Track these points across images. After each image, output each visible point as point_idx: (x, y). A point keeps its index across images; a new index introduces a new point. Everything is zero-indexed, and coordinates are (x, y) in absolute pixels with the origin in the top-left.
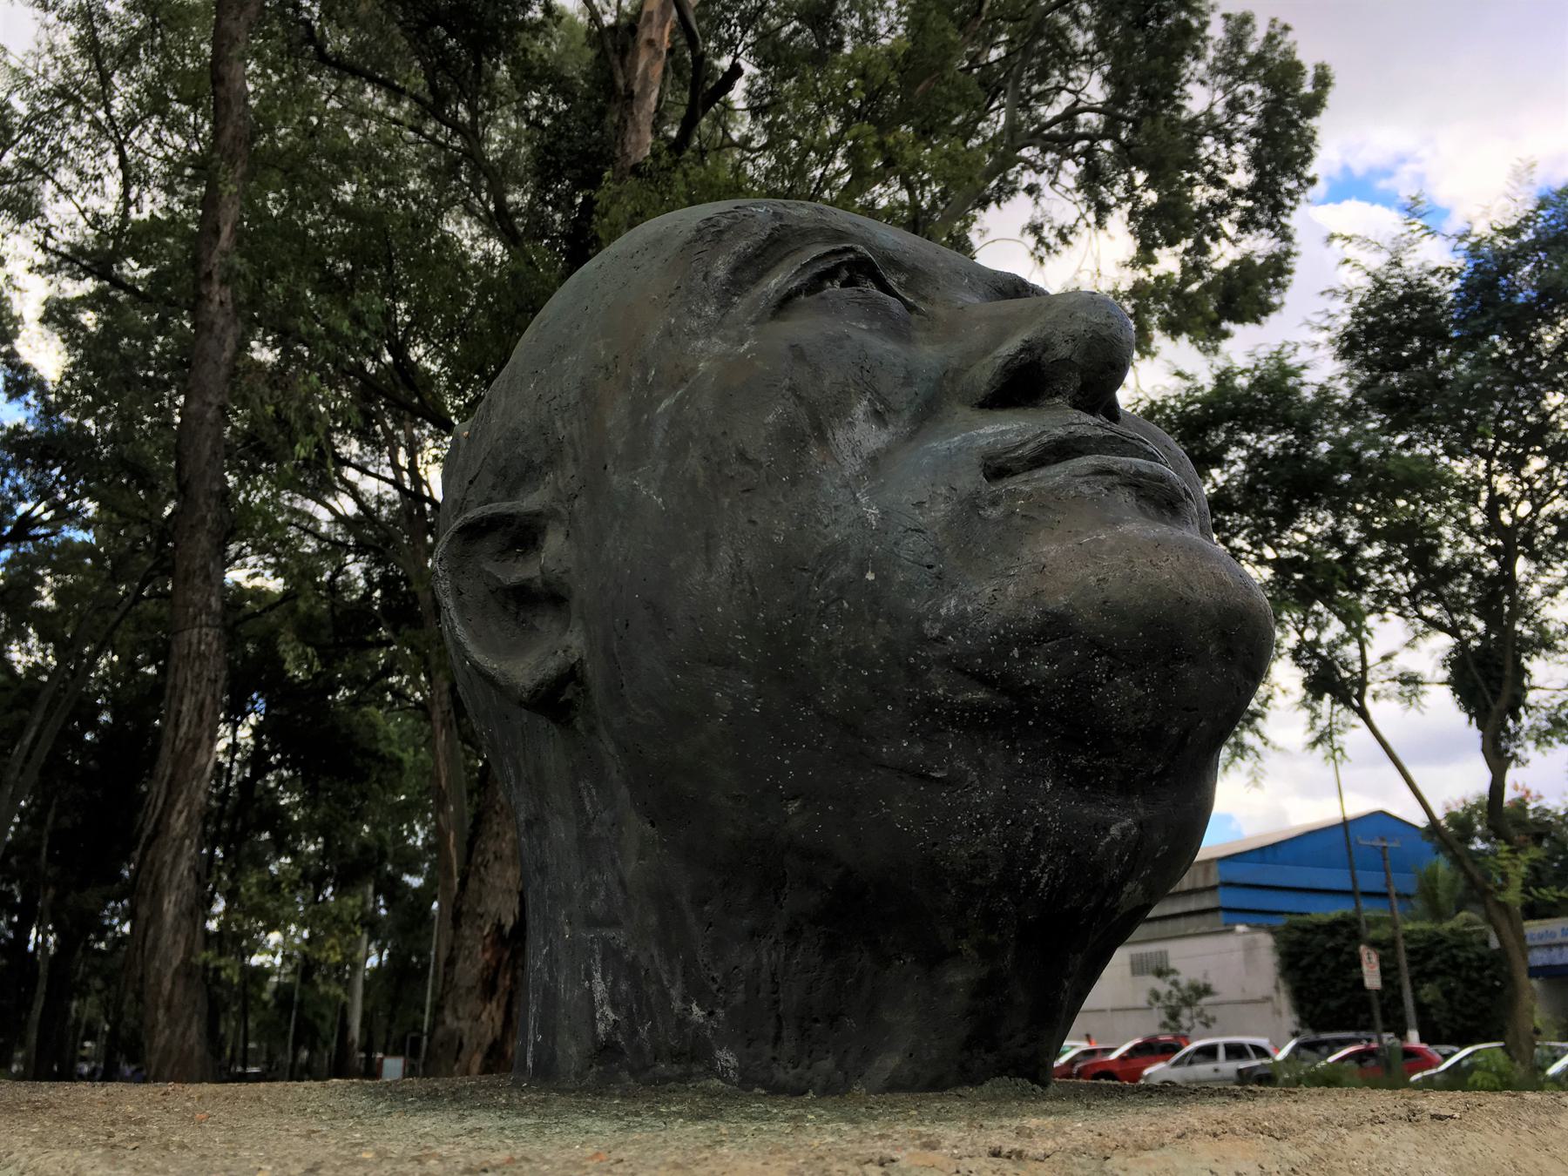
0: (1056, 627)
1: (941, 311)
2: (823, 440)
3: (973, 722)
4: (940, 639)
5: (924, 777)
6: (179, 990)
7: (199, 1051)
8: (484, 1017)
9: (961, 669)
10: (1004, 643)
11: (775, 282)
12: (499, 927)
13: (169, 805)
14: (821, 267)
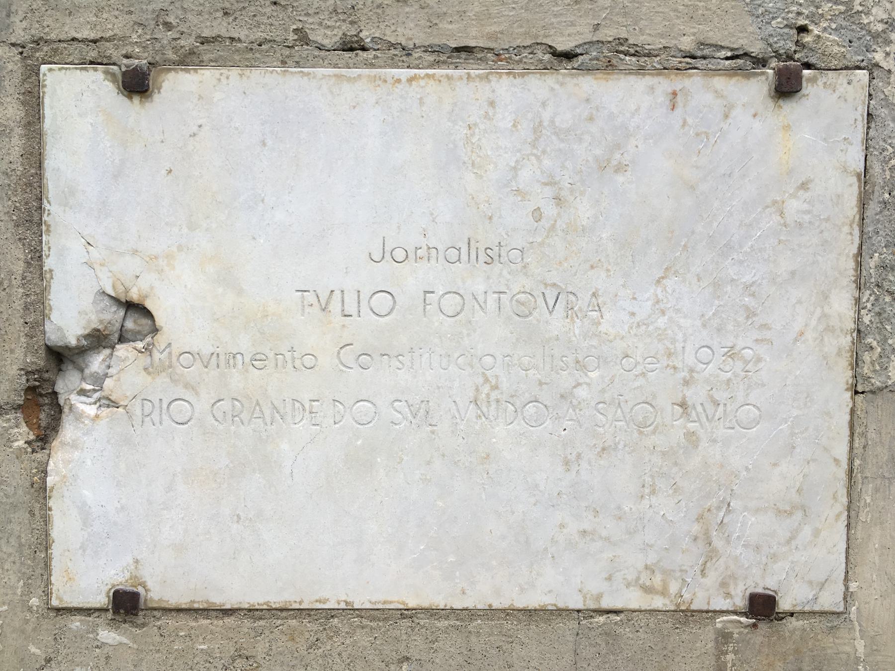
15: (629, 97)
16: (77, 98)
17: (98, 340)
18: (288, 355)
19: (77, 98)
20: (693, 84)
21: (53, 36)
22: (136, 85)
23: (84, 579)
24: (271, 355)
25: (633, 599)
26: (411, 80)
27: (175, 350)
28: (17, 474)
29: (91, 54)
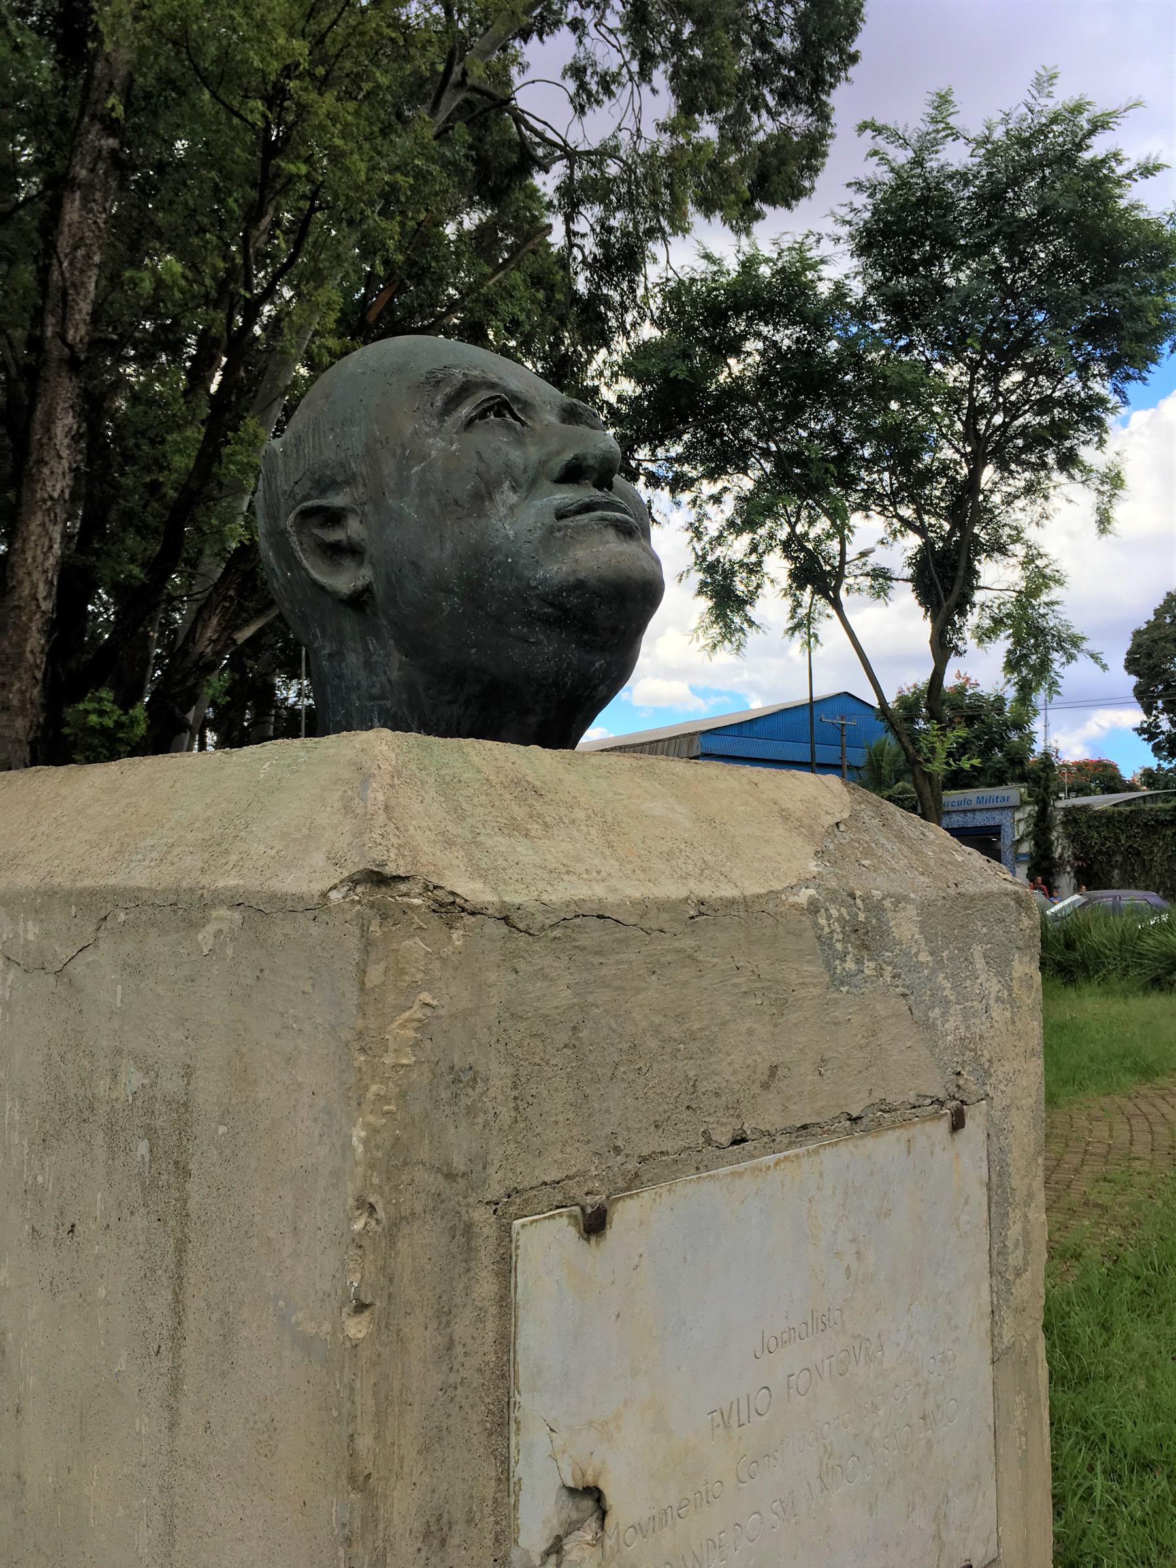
0: (580, 585)
1: (537, 426)
2: (491, 499)
3: (548, 622)
4: (536, 588)
5: (527, 641)
9: (544, 600)
10: (561, 590)
11: (465, 411)
14: (486, 405)
18: (703, 1489)
21: (526, 1184)
22: (594, 1224)
24: (691, 1496)
26: (777, 1164)
27: (622, 1528)
29: (553, 1196)
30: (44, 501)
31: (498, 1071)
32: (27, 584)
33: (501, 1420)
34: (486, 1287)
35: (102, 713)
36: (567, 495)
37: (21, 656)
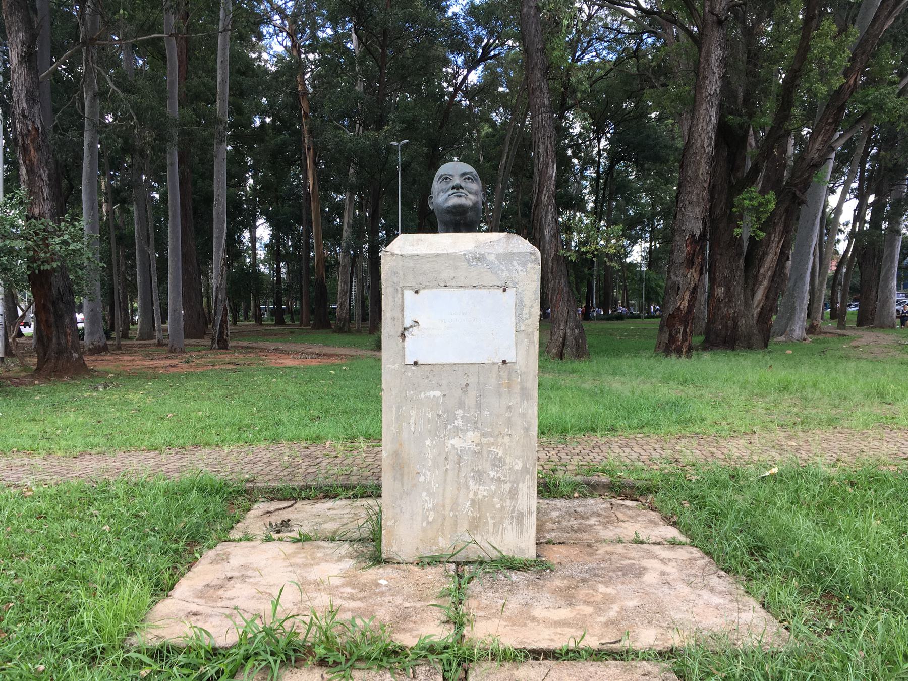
6: (555, 266)
7: (565, 289)
8: (689, 276)
12: (693, 235)
13: (540, 193)
15: (484, 292)
16: (409, 294)
17: (411, 327)
19: (409, 294)
20: (492, 290)
22: (417, 292)
23: (410, 360)
25: (486, 361)
28: (400, 345)
29: (411, 288)
30: (707, 97)
31: (401, 273)
32: (699, 141)
33: (402, 310)
34: (400, 296)
35: (751, 199)
36: (451, 192)
37: (697, 177)
